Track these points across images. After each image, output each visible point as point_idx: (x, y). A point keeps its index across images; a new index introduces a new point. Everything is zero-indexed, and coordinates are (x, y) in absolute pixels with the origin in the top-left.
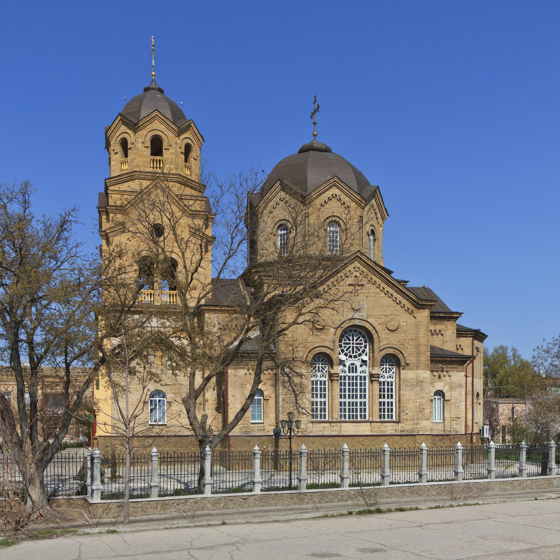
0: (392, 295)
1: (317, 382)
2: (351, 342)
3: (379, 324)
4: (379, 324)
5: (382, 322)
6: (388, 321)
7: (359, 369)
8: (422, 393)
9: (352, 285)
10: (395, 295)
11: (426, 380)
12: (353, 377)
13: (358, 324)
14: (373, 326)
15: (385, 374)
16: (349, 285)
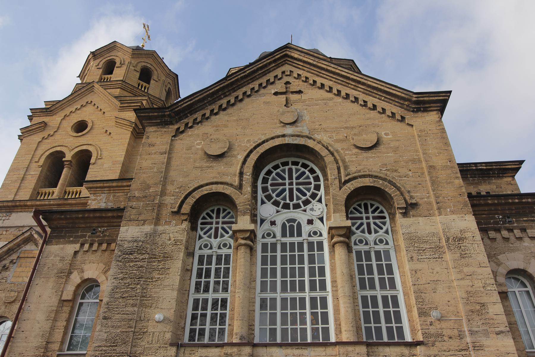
0: (356, 99)
1: (210, 257)
2: (287, 181)
3: (337, 141)
4: (337, 141)
5: (341, 137)
6: (355, 134)
7: (306, 229)
8: (467, 265)
9: (282, 93)
10: (362, 97)
11: (468, 235)
12: (292, 244)
13: (292, 142)
14: (323, 146)
15: (367, 235)
16: (276, 94)
